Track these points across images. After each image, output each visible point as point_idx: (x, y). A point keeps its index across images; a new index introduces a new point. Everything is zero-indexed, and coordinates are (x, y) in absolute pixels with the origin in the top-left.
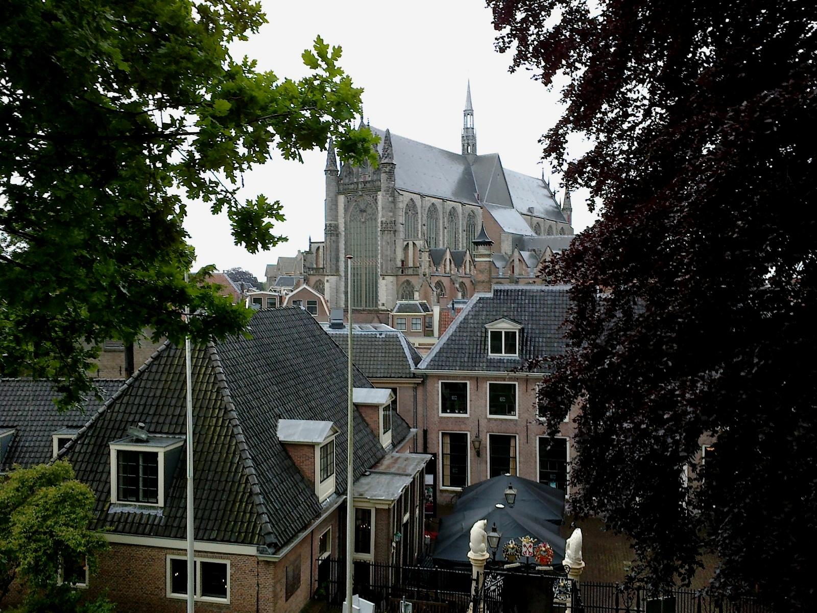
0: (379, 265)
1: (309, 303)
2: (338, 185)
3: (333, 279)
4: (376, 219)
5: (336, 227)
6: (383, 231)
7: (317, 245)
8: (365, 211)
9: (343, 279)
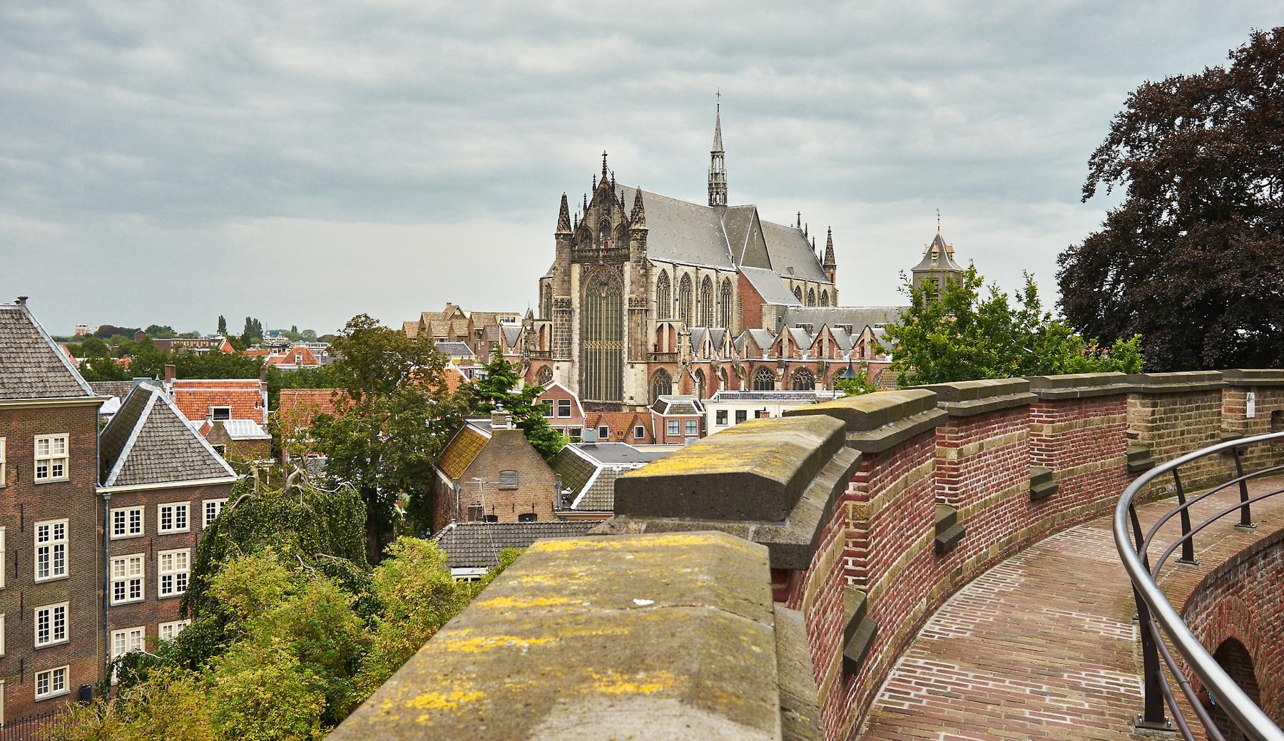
0: (626, 350)
1: (561, 402)
2: (573, 251)
3: (565, 366)
4: (621, 295)
5: (569, 302)
6: (631, 312)
7: (541, 323)
8: (606, 284)
9: (577, 365)
